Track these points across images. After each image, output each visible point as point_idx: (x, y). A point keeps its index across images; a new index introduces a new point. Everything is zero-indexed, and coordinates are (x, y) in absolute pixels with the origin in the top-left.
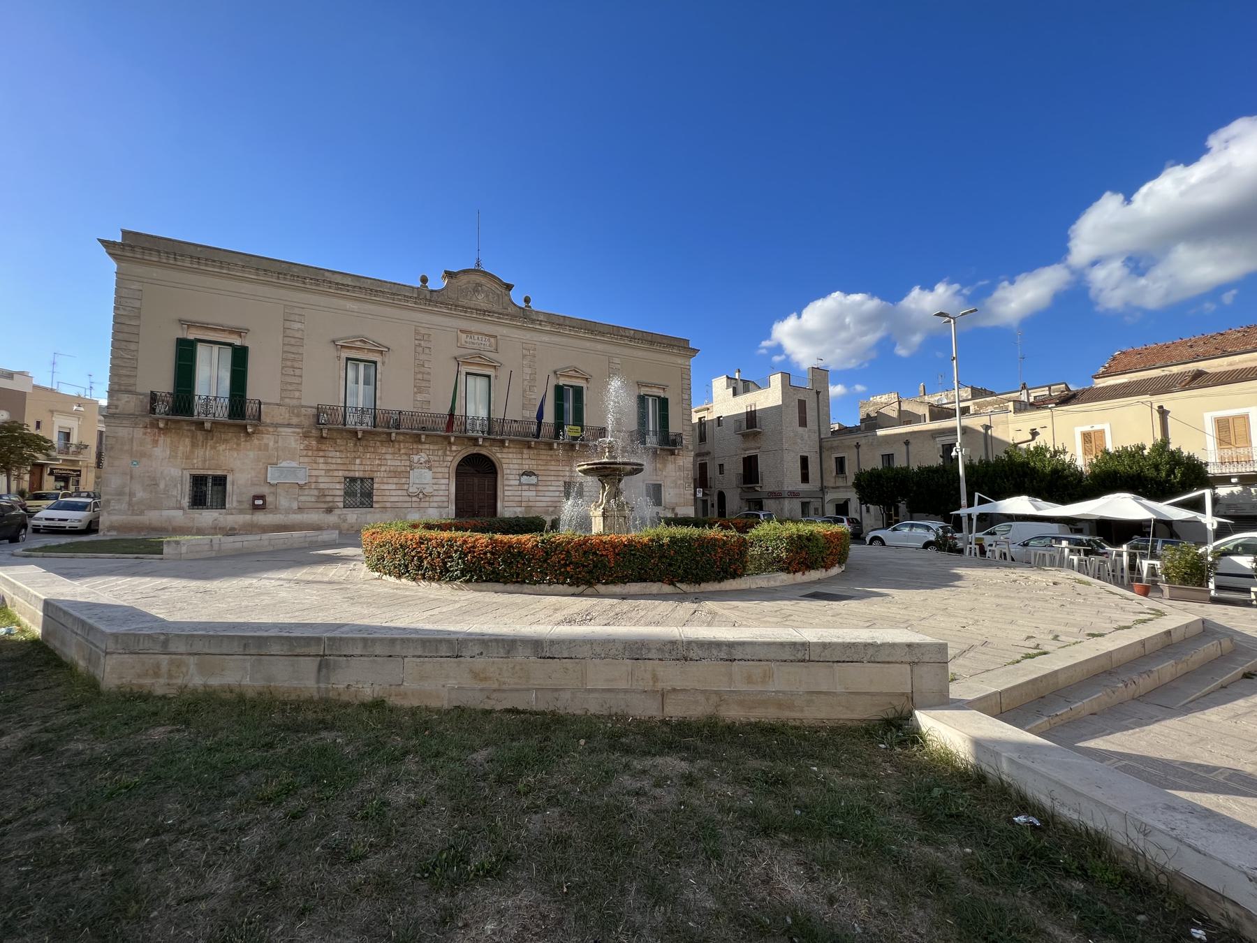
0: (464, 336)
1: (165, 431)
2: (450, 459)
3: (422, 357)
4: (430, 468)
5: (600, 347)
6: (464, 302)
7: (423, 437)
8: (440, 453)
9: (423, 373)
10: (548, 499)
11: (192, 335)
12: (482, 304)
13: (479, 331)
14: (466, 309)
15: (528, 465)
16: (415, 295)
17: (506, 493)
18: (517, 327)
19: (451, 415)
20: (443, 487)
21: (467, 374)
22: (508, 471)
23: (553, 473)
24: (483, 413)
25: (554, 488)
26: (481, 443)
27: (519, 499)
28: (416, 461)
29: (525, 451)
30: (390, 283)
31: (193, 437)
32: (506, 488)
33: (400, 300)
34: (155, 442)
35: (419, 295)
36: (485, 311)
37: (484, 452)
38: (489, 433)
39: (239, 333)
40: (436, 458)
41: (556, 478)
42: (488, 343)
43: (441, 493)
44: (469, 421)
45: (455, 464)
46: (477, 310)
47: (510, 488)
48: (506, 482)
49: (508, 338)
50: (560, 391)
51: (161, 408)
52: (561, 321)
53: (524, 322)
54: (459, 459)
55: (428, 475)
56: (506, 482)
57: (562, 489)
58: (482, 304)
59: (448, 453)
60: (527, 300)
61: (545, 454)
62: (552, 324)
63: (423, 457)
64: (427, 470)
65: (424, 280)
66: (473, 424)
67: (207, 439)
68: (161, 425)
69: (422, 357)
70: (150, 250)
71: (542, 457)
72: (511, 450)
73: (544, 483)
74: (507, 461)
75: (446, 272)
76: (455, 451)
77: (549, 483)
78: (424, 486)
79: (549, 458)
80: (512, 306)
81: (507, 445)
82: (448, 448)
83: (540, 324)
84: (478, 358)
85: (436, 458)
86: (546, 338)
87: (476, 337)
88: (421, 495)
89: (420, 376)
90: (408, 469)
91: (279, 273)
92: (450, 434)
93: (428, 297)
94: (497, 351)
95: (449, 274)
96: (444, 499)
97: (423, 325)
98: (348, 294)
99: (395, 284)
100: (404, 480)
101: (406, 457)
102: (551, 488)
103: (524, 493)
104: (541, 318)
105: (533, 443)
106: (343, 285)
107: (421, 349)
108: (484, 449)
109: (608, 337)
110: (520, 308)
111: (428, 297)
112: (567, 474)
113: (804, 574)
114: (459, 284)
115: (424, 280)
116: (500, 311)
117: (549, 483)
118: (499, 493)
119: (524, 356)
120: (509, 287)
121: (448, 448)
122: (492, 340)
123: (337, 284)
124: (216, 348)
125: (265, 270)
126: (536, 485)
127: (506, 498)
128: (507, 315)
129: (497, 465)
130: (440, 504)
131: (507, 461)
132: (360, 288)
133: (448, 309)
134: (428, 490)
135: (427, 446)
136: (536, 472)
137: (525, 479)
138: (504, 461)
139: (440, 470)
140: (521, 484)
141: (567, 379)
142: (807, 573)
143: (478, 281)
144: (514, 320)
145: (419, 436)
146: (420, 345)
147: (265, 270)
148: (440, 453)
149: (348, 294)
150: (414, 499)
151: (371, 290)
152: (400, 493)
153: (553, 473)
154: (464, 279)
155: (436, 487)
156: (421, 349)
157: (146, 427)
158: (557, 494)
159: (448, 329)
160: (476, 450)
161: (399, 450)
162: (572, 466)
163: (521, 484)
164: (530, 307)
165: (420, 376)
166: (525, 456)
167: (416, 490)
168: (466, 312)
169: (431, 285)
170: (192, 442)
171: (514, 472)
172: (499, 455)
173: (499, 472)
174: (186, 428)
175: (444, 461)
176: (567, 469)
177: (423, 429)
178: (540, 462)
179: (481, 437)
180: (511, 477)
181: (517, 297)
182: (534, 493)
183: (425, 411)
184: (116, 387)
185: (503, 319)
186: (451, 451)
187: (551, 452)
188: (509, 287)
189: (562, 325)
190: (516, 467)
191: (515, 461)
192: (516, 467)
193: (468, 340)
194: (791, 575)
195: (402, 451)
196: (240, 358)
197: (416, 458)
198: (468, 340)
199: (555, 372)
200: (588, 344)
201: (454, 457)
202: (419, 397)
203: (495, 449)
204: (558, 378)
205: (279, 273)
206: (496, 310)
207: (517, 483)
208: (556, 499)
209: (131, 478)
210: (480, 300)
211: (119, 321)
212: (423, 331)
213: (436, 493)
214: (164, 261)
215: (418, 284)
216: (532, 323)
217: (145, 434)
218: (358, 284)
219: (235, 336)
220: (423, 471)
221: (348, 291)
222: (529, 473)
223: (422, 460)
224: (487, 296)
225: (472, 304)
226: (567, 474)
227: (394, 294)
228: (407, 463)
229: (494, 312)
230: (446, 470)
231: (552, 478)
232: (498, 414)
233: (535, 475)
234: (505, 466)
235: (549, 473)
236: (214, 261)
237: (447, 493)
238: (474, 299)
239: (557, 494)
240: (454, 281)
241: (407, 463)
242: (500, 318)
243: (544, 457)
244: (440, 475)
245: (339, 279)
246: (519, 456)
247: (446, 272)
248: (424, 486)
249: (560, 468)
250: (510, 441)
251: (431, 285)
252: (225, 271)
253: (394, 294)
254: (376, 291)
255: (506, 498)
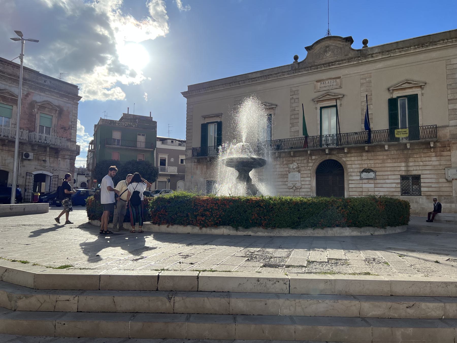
0: (319, 84)
1: (199, 162)
2: (311, 164)
3: (294, 105)
4: (299, 171)
5: (434, 55)
6: (318, 62)
7: (292, 153)
8: (305, 161)
9: (295, 115)
10: (385, 190)
11: (207, 121)
12: (330, 59)
13: (328, 77)
14: (317, 66)
15: (367, 164)
16: (290, 70)
17: (351, 186)
18: (354, 65)
19: (306, 136)
20: (308, 183)
21: (321, 108)
22: (351, 170)
23: (389, 169)
24: (334, 132)
25: (392, 181)
26: (327, 152)
27: (361, 190)
28: (291, 168)
29: (364, 154)
30: (277, 68)
31: (207, 165)
32: (350, 182)
33: (280, 76)
34: (197, 168)
35: (292, 68)
36: (329, 63)
37: (334, 158)
38: (337, 144)
39: (218, 116)
40: (303, 165)
41: (392, 173)
42: (335, 84)
43: (306, 186)
44: (323, 139)
45: (315, 167)
46: (323, 64)
47: (353, 182)
48: (350, 178)
49: (349, 76)
50: (393, 103)
51: (196, 154)
52: (395, 46)
53: (360, 60)
54: (317, 164)
55: (298, 175)
56: (350, 178)
57: (399, 181)
58: (330, 59)
59: (310, 161)
60: (365, 42)
61: (381, 155)
62: (382, 53)
63: (295, 165)
64: (297, 173)
65: (296, 58)
66: (327, 140)
67: (198, 164)
68: (196, 161)
69: (294, 105)
70: (193, 91)
71: (378, 157)
72: (352, 155)
73: (381, 177)
74: (350, 162)
75: (306, 48)
76: (314, 159)
77: (386, 177)
78: (296, 182)
79: (385, 157)
80: (351, 52)
81: (346, 151)
82: (310, 158)
83: (372, 57)
84: (327, 96)
85: (303, 165)
86: (380, 65)
87: (327, 82)
88: (294, 188)
89: (293, 117)
90: (288, 172)
91: (230, 83)
92: (306, 149)
93: (297, 67)
94: (341, 87)
95: (308, 48)
96: (308, 190)
97: (295, 85)
98: (257, 82)
99: (279, 67)
100: (286, 179)
101: (286, 166)
102: (388, 181)
103: (364, 186)
104: (376, 51)
105: (366, 148)
106: (254, 78)
107: (293, 100)
108: (333, 156)
109: (441, 44)
110: (358, 50)
111: (297, 67)
112: (403, 169)
113: (168, 227)
114: (315, 52)
115: (296, 58)
116: (343, 58)
117: (386, 177)
118: (346, 186)
119: (362, 84)
120: (350, 40)
121: (310, 158)
122: (338, 80)
123: (251, 79)
124: (213, 124)
125: (225, 84)
126: (375, 179)
127: (350, 190)
128: (345, 60)
129: (343, 166)
130: (306, 193)
131: (350, 162)
132: (261, 77)
133: (307, 71)
134: (298, 185)
135: (297, 158)
136: (373, 169)
137: (364, 175)
138: (348, 163)
139: (305, 172)
140: (361, 179)
141: (400, 92)
142: (170, 226)
143: (327, 45)
144: (351, 62)
145: (290, 152)
146: (292, 98)
147: (225, 84)
148: (305, 161)
149: (257, 82)
150: (291, 190)
151: (266, 76)
152: (284, 187)
153: (389, 169)
154: (318, 47)
155: (303, 183)
156: (293, 100)
157: (194, 162)
158: (394, 185)
159: (309, 83)
160: (328, 157)
161: (283, 162)
162: (407, 161)
163: (361, 179)
164: (367, 47)
165: (293, 117)
166: (364, 158)
167: (292, 185)
168: (317, 68)
169: (299, 61)
170: (207, 167)
171: (356, 170)
172: (344, 159)
173: (345, 170)
174: (205, 161)
175: (307, 167)
176: (403, 164)
177: (292, 148)
178: (377, 161)
179: (326, 148)
180: (353, 174)
181: (357, 45)
182: (373, 185)
183: (296, 137)
184: (187, 148)
185: (343, 63)
186: (312, 160)
187: (386, 153)
188: (350, 40)
189: (391, 50)
190: (358, 166)
191: (356, 162)
192: (358, 166)
193: (322, 85)
194: (156, 226)
195: (285, 163)
196: (220, 125)
197: (291, 166)
198: (322, 85)
199: (389, 89)
200: (422, 57)
201: (314, 163)
202: (293, 129)
203: (341, 155)
204: (392, 93)
205: (230, 83)
206: (340, 59)
207: (359, 178)
208: (394, 190)
209: (191, 183)
210: (329, 57)
211: (188, 122)
212: (294, 89)
213: (303, 187)
214: (197, 93)
215: (292, 61)
216: (366, 58)
217: (194, 165)
218: (262, 75)
219: (218, 118)
220: (296, 173)
221: (257, 80)
222: (367, 171)
223: (295, 167)
224: (333, 52)
225: (323, 62)
226: (403, 169)
227: (277, 74)
228: (287, 169)
229: (335, 62)
230: (309, 172)
231: (389, 173)
232: (344, 130)
233: (372, 171)
234: (349, 166)
235: (386, 169)
236: (209, 87)
237: (309, 186)
238: (324, 58)
239: (394, 185)
240: (312, 51)
241: (287, 169)
242: (341, 64)
243: (381, 157)
244: (305, 175)
245: (254, 76)
246: (359, 158)
247: (306, 48)
248: (296, 182)
249: (396, 164)
250: (349, 148)
251: (299, 61)
252: (213, 90)
253: (277, 74)
254: (268, 75)
255: (350, 190)
